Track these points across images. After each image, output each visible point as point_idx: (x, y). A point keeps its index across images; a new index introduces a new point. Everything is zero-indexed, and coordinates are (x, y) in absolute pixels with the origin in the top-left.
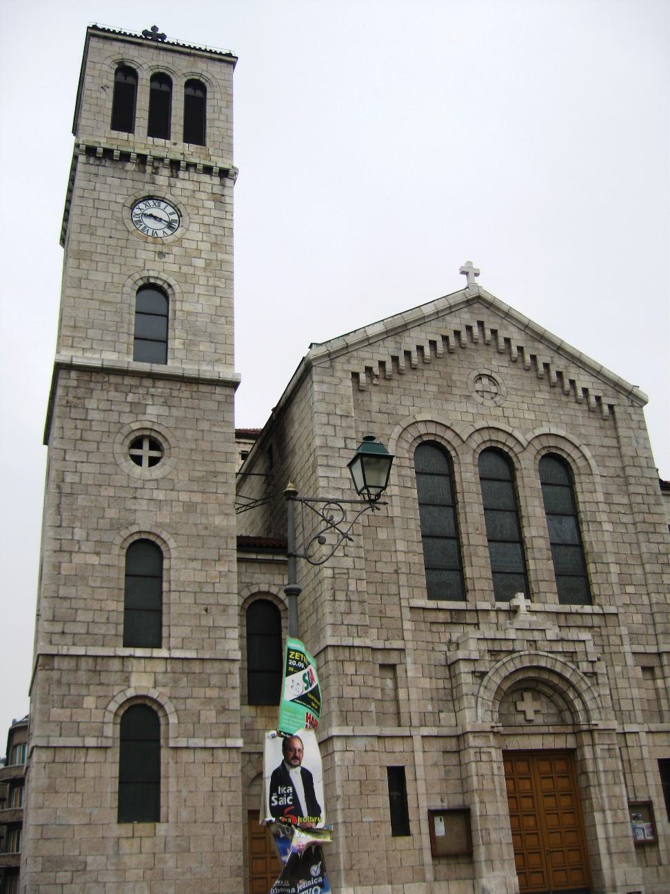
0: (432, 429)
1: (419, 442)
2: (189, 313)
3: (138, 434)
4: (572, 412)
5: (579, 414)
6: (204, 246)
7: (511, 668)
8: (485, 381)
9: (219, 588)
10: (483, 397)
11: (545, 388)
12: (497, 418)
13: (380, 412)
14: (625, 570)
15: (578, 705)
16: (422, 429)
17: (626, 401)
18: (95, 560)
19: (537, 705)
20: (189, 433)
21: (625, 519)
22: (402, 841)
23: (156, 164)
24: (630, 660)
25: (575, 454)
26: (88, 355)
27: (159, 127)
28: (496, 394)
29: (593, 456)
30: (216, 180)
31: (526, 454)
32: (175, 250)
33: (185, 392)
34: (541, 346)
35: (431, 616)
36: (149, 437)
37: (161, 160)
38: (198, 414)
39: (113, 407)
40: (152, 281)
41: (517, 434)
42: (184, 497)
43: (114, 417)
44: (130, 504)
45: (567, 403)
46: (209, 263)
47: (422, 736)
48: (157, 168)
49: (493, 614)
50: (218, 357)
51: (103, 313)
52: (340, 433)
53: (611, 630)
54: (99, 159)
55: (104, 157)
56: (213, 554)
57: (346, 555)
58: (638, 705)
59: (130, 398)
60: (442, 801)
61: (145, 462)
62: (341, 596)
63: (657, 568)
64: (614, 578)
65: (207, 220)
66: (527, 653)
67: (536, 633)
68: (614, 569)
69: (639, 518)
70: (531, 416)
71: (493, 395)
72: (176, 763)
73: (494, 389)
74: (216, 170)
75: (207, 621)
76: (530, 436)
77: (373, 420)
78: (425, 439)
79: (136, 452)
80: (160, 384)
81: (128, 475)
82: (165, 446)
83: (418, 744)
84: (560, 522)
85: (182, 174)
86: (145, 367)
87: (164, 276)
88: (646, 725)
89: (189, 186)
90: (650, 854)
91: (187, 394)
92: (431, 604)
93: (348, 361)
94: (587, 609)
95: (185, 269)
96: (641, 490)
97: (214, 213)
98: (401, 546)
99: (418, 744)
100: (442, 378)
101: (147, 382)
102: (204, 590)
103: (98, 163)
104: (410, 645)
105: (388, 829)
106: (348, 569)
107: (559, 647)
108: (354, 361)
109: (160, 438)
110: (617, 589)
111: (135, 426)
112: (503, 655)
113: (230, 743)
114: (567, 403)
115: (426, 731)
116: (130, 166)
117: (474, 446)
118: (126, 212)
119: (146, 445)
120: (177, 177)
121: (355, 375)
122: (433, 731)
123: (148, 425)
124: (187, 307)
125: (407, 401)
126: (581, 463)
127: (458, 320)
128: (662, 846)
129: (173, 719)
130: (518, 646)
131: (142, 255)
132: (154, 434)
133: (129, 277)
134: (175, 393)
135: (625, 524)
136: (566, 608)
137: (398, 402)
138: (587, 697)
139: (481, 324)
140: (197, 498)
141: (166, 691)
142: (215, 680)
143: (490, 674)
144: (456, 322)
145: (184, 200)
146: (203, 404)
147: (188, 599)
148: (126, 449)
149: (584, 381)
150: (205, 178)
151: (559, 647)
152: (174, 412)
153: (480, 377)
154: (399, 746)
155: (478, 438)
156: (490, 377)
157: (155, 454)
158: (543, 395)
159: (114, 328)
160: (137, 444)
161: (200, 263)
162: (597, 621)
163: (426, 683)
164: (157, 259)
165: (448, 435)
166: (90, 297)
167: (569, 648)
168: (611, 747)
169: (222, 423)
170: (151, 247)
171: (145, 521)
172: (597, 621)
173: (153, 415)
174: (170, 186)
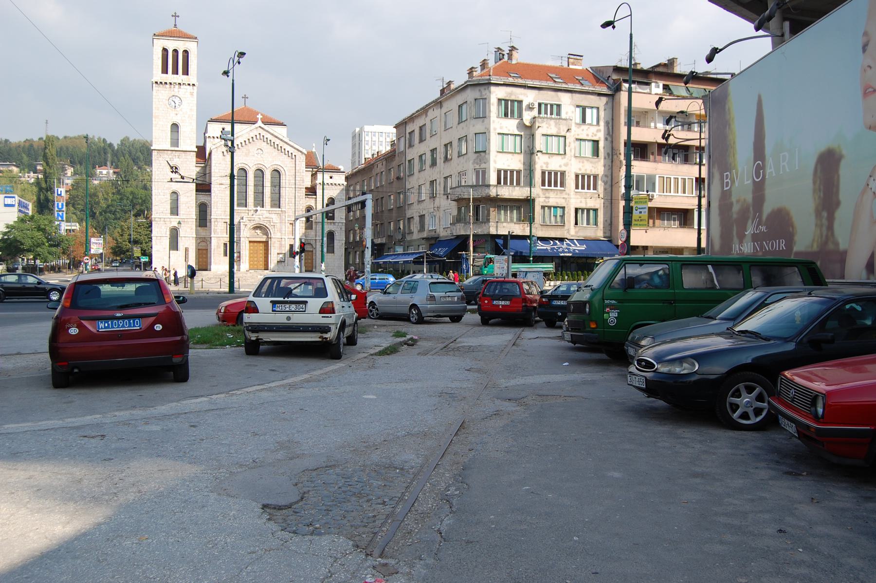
0: (243, 165)
16: (240, 165)
18: (163, 197)
25: (282, 170)
27: (175, 72)
30: (191, 87)
33: (183, 154)
59: (170, 157)
73: (261, 152)
76: (269, 165)
86: (173, 149)
116: (168, 86)
126: (283, 172)
139: (260, 134)
146: (188, 157)
147: (184, 205)
152: (181, 160)
155: (255, 167)
158: (275, 152)
165: (247, 167)
174: (178, 91)
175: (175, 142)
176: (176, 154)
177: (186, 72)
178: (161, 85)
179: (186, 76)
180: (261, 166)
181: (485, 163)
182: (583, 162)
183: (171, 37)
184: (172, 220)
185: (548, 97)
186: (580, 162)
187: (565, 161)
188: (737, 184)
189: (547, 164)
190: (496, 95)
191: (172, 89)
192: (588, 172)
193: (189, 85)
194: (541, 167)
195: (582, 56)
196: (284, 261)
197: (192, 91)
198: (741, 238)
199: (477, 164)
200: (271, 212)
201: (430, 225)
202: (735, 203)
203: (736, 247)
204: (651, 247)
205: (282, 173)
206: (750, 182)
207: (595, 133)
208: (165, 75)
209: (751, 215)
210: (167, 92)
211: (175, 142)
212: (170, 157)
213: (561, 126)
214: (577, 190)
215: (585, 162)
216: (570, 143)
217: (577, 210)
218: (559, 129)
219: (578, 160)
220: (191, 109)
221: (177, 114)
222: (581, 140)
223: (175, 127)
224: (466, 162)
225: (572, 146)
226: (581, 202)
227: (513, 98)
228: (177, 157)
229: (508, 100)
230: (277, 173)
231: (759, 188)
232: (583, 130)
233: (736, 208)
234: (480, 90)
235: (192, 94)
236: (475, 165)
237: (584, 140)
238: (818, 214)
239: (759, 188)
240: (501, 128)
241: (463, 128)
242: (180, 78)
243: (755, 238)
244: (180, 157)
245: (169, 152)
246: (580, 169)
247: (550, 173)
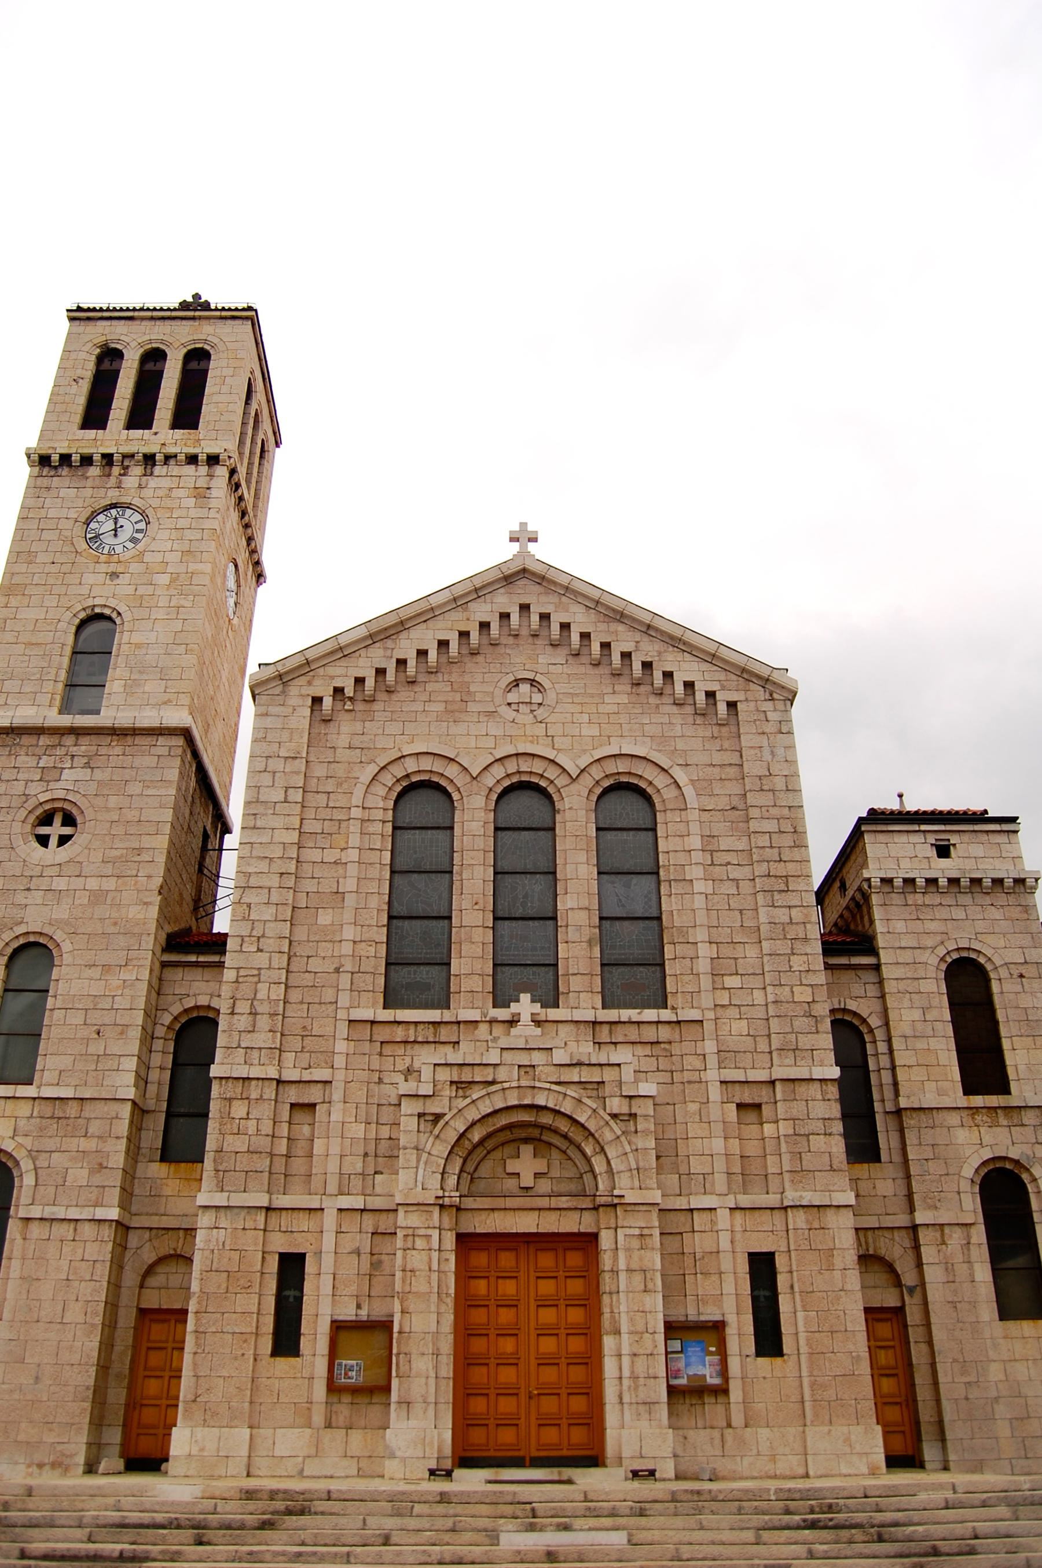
0: (426, 764)
1: (404, 784)
2: (139, 646)
3: (47, 807)
4: (666, 719)
5: (678, 720)
6: (173, 557)
7: (486, 1108)
8: (525, 688)
9: (121, 1003)
10: (518, 711)
11: (624, 686)
12: (535, 739)
13: (350, 748)
14: (726, 951)
15: (599, 1165)
16: (411, 765)
17: (761, 694)
19: (541, 1165)
20: (113, 801)
21: (735, 873)
22: (283, 1363)
23: (126, 463)
24: (715, 1093)
25: (660, 781)
28: (540, 704)
30: (203, 470)
31: (574, 787)
32: (134, 567)
34: (621, 628)
36: (63, 809)
37: (132, 456)
38: (128, 774)
39: (20, 776)
40: (97, 610)
42: (93, 884)
43: (19, 788)
44: (20, 898)
45: (657, 706)
46: (175, 578)
47: (340, 1210)
48: (128, 467)
49: (483, 1028)
50: (166, 697)
51: (27, 658)
52: (280, 781)
53: (687, 1047)
54: (56, 467)
55: (61, 465)
56: (119, 958)
57: (259, 950)
58: (720, 1165)
60: (359, 1307)
62: (243, 1007)
63: (783, 947)
64: (703, 965)
65: (182, 523)
66: (514, 1084)
67: (535, 1054)
68: (705, 951)
69: (761, 869)
70: (588, 731)
71: (535, 707)
72: (24, 1239)
73: (537, 698)
74: (202, 457)
77: (337, 759)
78: (415, 779)
79: (44, 830)
80: (85, 740)
81: (24, 861)
82: (79, 820)
83: (330, 1220)
84: (627, 886)
85: (158, 470)
87: (112, 603)
88: (731, 1197)
89: (166, 483)
90: (713, 1409)
91: (118, 750)
92: (388, 1015)
93: (309, 683)
96: (771, 826)
97: (193, 513)
98: (349, 933)
99: (330, 1220)
100: (453, 690)
101: (69, 740)
102: (100, 1006)
103: (52, 473)
104: (340, 1076)
105: (267, 1344)
106: (259, 969)
107: (574, 1075)
108: (317, 682)
109: (75, 811)
110: (706, 982)
111: (43, 798)
112: (476, 1087)
113: (100, 1213)
114: (657, 706)
115: (345, 1202)
116: (94, 471)
117: (490, 781)
118: (79, 530)
119: (58, 820)
120: (151, 474)
121: (317, 701)
122: (358, 1202)
123: (61, 794)
124: (136, 638)
125: (393, 728)
126: (670, 793)
127: (488, 607)
128: (736, 1393)
129: (29, 1180)
130: (502, 1074)
131: (89, 579)
132: (67, 806)
133: (68, 609)
134: (103, 751)
135: (736, 881)
136: (612, 1015)
137: (380, 731)
138: (611, 1152)
139: (525, 608)
141: (28, 1142)
142: (94, 1128)
143: (447, 1118)
144: (483, 611)
145: (155, 503)
146: (138, 762)
148: (28, 828)
149: (686, 669)
151: (574, 1075)
152: (98, 775)
153: (517, 683)
154: (303, 1223)
155: (498, 771)
156: (532, 682)
157: (67, 831)
158: (620, 697)
159: (38, 676)
160: (46, 820)
161: (164, 579)
162: (664, 1033)
163: (358, 1130)
164: (108, 582)
165: (451, 771)
166: (14, 640)
167: (595, 1076)
168: (646, 1232)
169: (160, 784)
170: (103, 568)
172: (664, 1033)
174: (140, 487)
178: (65, 471)
191: (113, 481)
193: (192, 459)
196: (722, 1391)
197: (202, 483)
210: (88, 492)
235: (201, 494)
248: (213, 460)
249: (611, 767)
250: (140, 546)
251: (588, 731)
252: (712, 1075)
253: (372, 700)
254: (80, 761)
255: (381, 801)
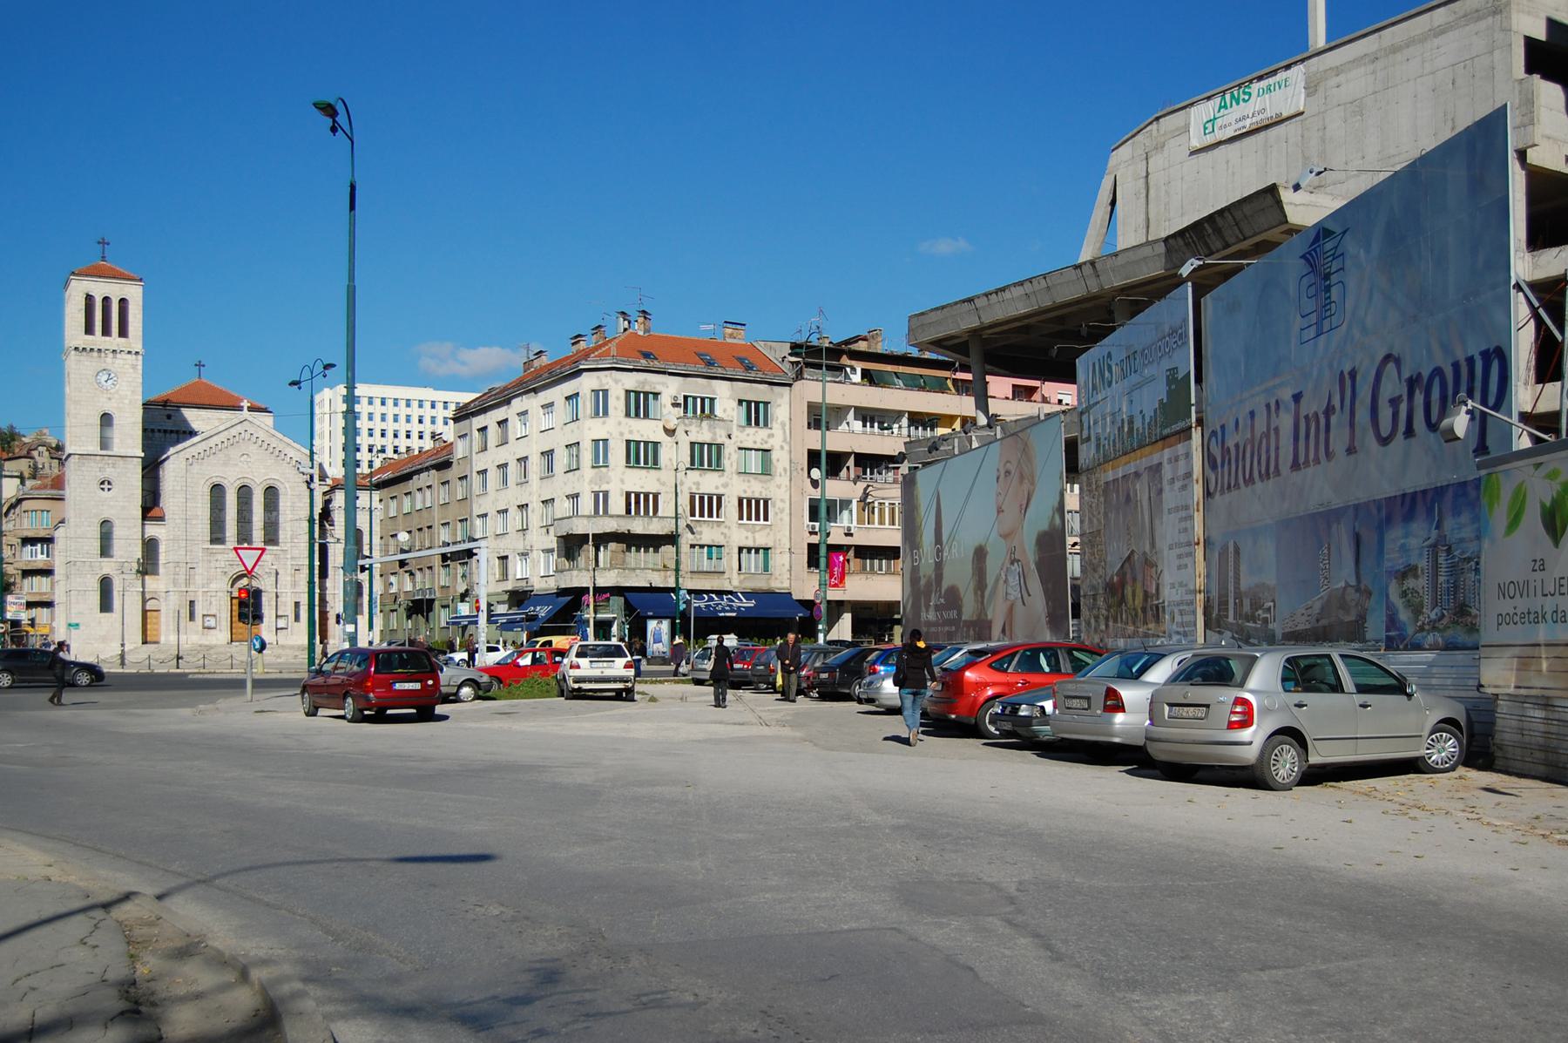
0: (219, 479)
6: (129, 393)
12: (248, 473)
18: (88, 529)
24: (290, 567)
26: (82, 448)
27: (106, 331)
29: (290, 487)
30: (134, 356)
32: (116, 396)
33: (120, 462)
35: (211, 551)
41: (256, 480)
42: (121, 504)
46: (130, 402)
59: (99, 465)
61: (106, 490)
64: (289, 536)
68: (290, 533)
70: (263, 471)
75: (131, 549)
79: (102, 486)
82: (113, 484)
89: (122, 362)
94: (275, 548)
95: (121, 405)
101: (106, 458)
116: (95, 354)
119: (106, 483)
140: (126, 504)
145: (119, 370)
150: (129, 356)
152: (118, 470)
155: (238, 482)
157: (109, 487)
160: (102, 483)
161: (127, 401)
165: (226, 482)
170: (105, 396)
171: (105, 515)
173: (109, 473)
175: (105, 443)
176: (110, 462)
177: (123, 333)
179: (123, 340)
180: (242, 481)
181: (608, 483)
182: (749, 481)
183: (100, 277)
184: (103, 564)
185: (698, 387)
186: (744, 481)
187: (724, 480)
188: (923, 561)
189: (698, 484)
190: (623, 385)
192: (757, 495)
193: (129, 352)
194: (690, 488)
195: (744, 325)
198: (928, 607)
199: (596, 484)
200: (210, 551)
201: (518, 569)
202: (922, 578)
203: (923, 615)
204: (849, 601)
205: (281, 491)
206: (932, 561)
207: (766, 438)
208: (90, 337)
209: (934, 589)
211: (105, 443)
212: (99, 465)
213: (717, 430)
214: (741, 522)
215: (752, 481)
216: (730, 454)
217: (740, 549)
218: (715, 434)
219: (743, 477)
220: (133, 392)
221: (110, 399)
222: (745, 449)
223: (106, 420)
224: (578, 480)
225: (731, 458)
226: (747, 538)
227: (647, 389)
228: (111, 465)
229: (640, 392)
230: (271, 493)
231: (939, 566)
232: (748, 435)
233: (923, 582)
234: (598, 377)
235: (134, 367)
236: (593, 486)
237: (751, 449)
238: (976, 594)
239: (939, 566)
240: (631, 432)
241: (572, 431)
242: (114, 341)
243: (937, 608)
244: (117, 466)
245: (98, 458)
246: (745, 492)
247: (702, 499)
248: (137, 353)
249: (268, 482)
250: (117, 388)
251: (263, 471)
252: (289, 563)
253: (203, 459)
254: (111, 465)
255: (207, 490)
